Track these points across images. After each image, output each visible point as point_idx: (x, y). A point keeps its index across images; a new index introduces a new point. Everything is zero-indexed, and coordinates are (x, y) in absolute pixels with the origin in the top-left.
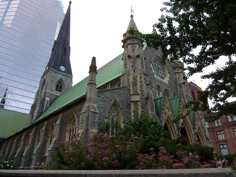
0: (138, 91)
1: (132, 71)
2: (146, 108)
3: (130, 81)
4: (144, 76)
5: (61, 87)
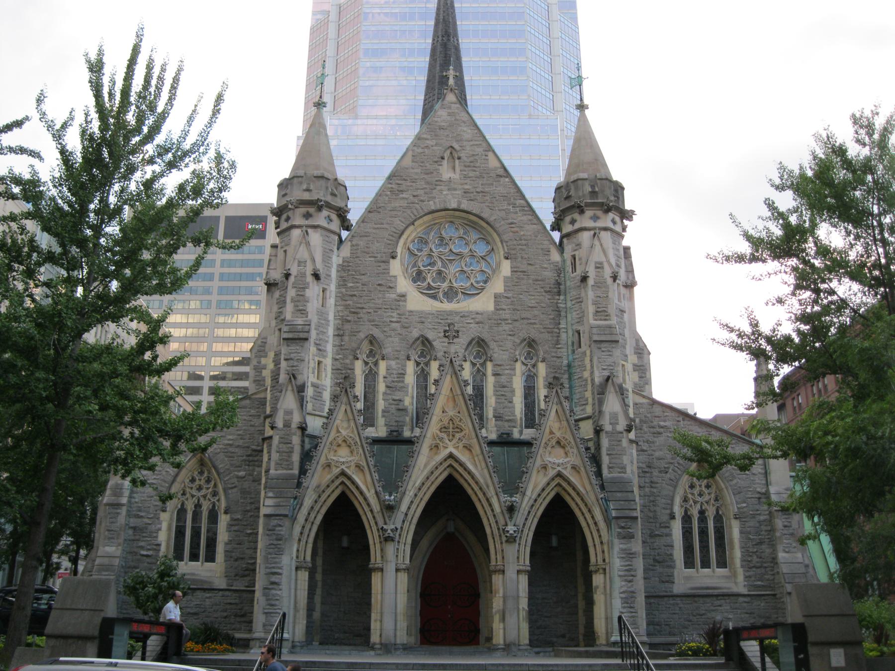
4: (288, 346)
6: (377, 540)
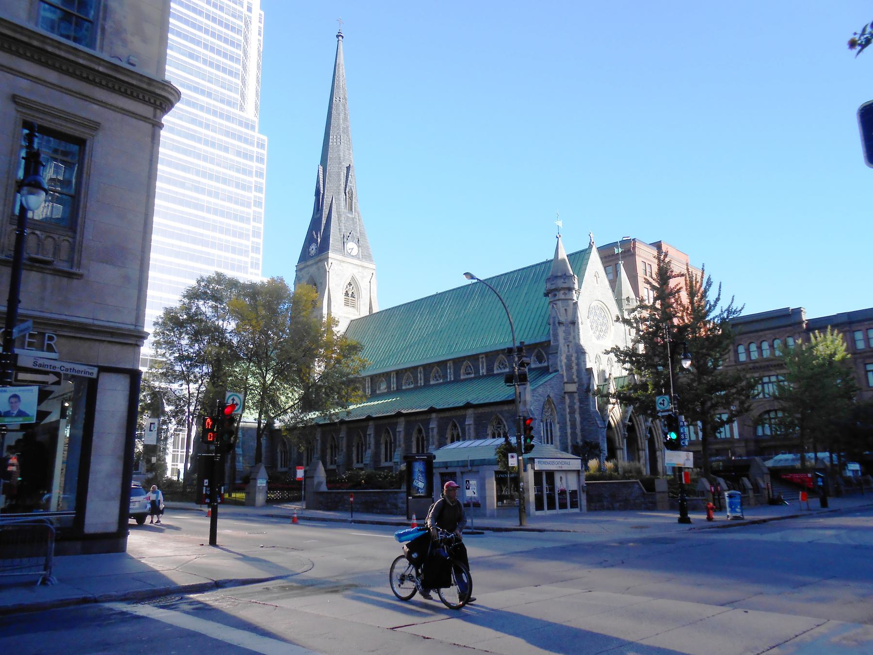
0: (574, 377)
1: (564, 346)
2: (586, 403)
3: (563, 363)
5: (353, 296)
6: (620, 438)
